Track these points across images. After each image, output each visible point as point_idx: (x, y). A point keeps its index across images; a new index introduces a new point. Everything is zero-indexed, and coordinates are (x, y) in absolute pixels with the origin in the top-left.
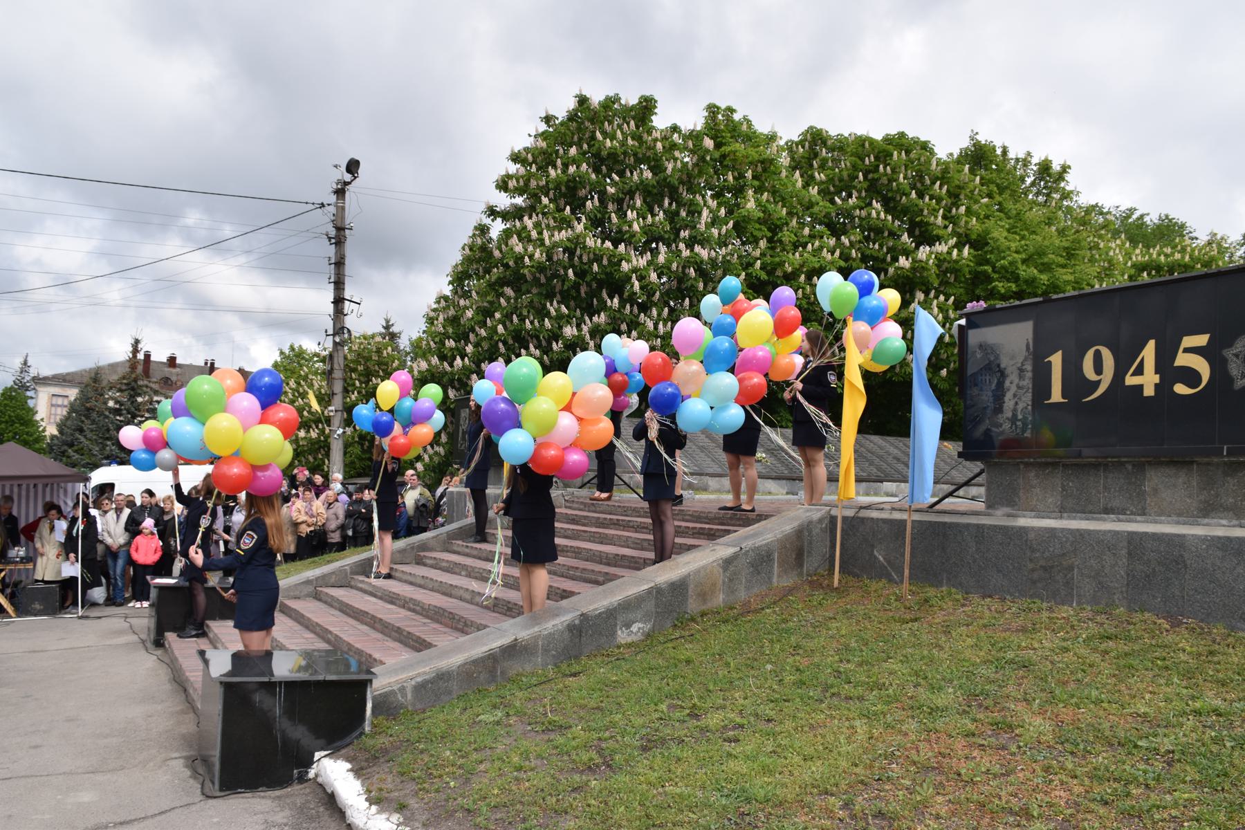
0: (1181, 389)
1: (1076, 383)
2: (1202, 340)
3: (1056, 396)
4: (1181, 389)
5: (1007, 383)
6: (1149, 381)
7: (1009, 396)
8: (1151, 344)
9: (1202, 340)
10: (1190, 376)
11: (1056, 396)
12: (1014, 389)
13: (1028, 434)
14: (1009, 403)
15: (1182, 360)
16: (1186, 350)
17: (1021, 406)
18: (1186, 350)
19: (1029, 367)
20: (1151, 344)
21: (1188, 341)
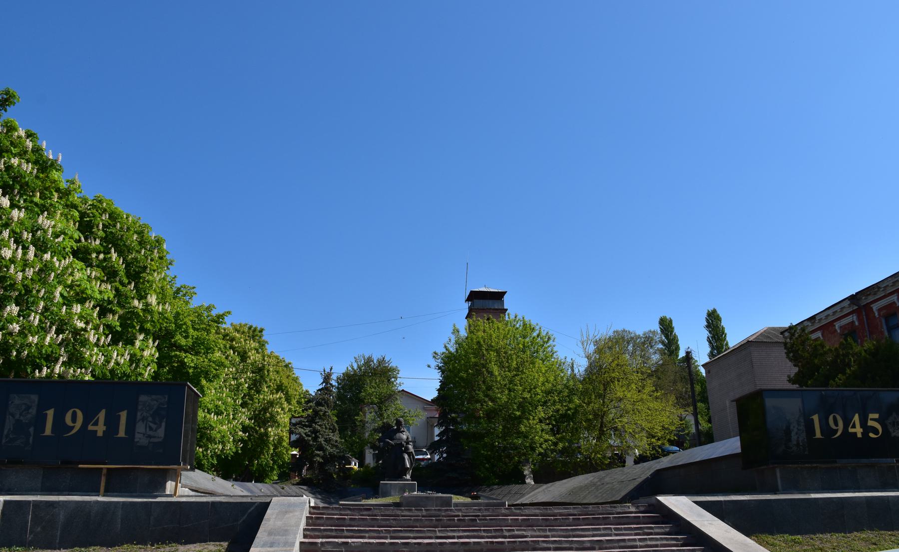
0: (872, 435)
1: (828, 431)
2: (876, 416)
3: (818, 435)
4: (872, 435)
5: (792, 428)
6: (858, 430)
7: (793, 434)
8: (857, 416)
9: (876, 416)
10: (875, 431)
11: (818, 435)
12: (795, 430)
13: (806, 453)
14: (794, 437)
15: (870, 423)
16: (871, 419)
17: (801, 439)
18: (871, 419)
19: (802, 420)
20: (857, 416)
21: (871, 416)
